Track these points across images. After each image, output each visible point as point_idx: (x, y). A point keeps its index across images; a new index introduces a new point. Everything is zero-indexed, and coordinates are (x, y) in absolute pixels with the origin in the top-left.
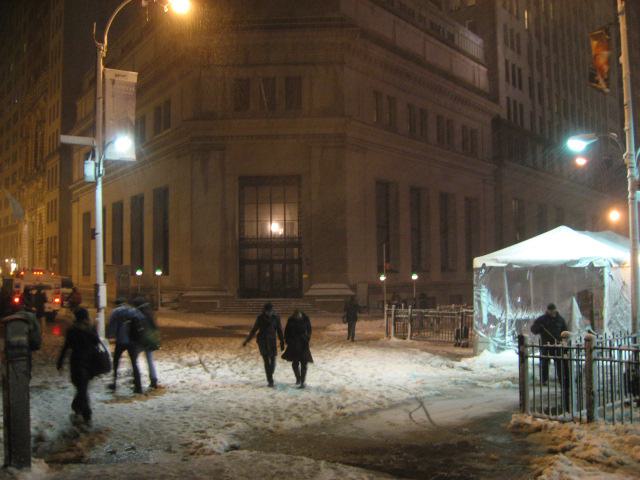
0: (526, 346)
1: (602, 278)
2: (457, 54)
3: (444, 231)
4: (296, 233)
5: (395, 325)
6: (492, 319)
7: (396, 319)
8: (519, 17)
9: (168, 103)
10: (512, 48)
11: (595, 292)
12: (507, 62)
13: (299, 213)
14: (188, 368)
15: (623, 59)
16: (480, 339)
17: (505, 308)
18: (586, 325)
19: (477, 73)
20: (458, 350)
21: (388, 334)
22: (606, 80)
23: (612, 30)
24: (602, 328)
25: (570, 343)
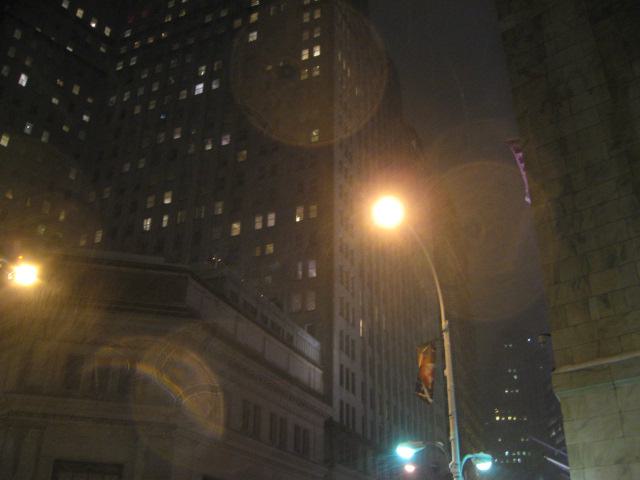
8: (355, 325)
10: (347, 353)
12: (342, 366)
15: (448, 372)
22: (431, 392)
23: (438, 346)
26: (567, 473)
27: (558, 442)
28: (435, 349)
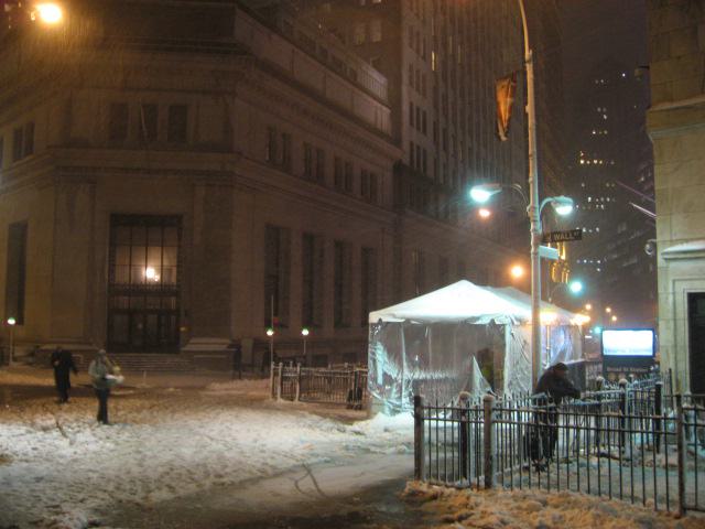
0: (423, 408)
1: (503, 336)
2: (360, 93)
3: (339, 286)
4: (174, 280)
5: (282, 384)
6: (388, 379)
7: (283, 379)
8: (426, 58)
9: (31, 126)
10: (418, 90)
11: (496, 351)
12: (411, 104)
13: (178, 257)
14: (42, 433)
15: (529, 109)
16: (374, 402)
17: (401, 366)
18: (486, 386)
19: (379, 112)
20: (351, 413)
21: (274, 395)
23: (518, 78)
24: (502, 389)
25: (468, 405)
26: (654, 221)
27: (646, 188)
28: (515, 82)
